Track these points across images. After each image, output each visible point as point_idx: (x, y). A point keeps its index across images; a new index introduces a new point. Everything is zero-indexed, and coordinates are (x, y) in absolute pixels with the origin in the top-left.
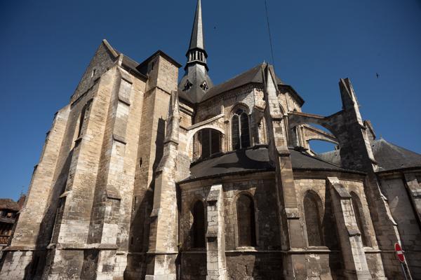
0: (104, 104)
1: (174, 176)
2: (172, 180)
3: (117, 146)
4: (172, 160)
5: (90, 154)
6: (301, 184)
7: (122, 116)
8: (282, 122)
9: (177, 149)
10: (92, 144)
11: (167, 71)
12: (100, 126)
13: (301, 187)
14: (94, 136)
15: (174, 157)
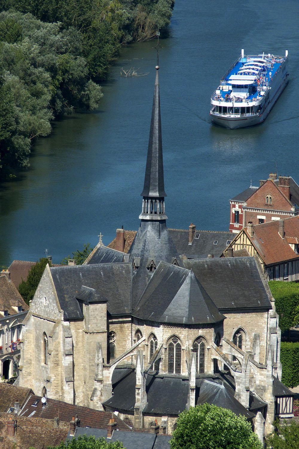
0: (57, 354)
1: (100, 400)
2: (99, 403)
3: (68, 385)
4: (99, 391)
5: (55, 388)
6: (149, 419)
7: (69, 364)
8: (140, 390)
9: (101, 384)
10: (55, 382)
11: (97, 313)
12: (57, 369)
13: (149, 420)
14: (56, 376)
15: (100, 389)
